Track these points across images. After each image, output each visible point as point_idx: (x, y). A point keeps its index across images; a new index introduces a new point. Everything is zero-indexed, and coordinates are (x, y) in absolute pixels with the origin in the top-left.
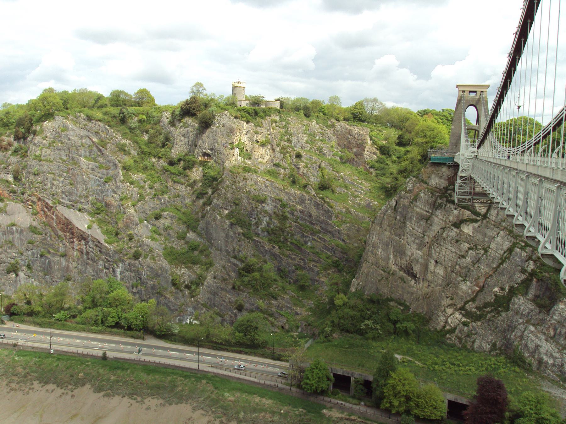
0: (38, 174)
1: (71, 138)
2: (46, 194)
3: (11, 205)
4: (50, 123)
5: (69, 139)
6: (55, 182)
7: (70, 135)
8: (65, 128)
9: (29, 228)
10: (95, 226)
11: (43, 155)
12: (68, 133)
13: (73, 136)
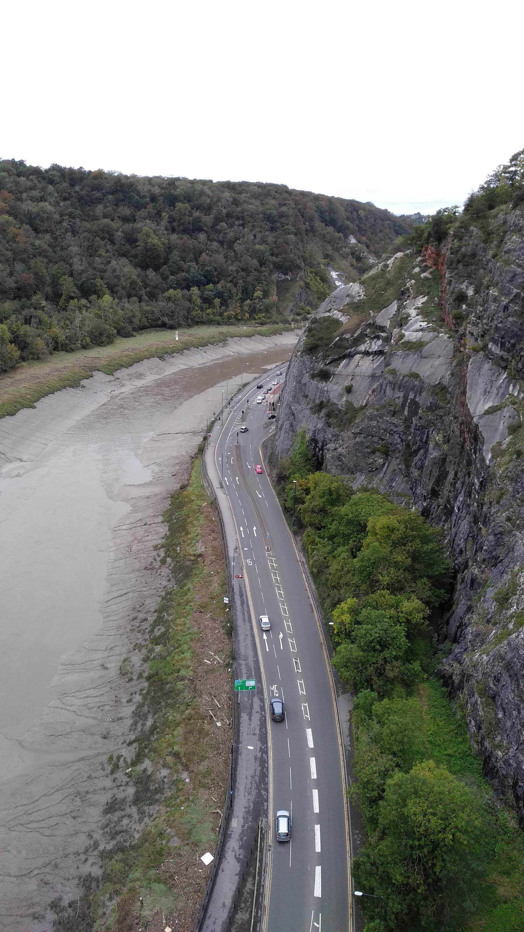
9: (435, 386)
10: (507, 412)
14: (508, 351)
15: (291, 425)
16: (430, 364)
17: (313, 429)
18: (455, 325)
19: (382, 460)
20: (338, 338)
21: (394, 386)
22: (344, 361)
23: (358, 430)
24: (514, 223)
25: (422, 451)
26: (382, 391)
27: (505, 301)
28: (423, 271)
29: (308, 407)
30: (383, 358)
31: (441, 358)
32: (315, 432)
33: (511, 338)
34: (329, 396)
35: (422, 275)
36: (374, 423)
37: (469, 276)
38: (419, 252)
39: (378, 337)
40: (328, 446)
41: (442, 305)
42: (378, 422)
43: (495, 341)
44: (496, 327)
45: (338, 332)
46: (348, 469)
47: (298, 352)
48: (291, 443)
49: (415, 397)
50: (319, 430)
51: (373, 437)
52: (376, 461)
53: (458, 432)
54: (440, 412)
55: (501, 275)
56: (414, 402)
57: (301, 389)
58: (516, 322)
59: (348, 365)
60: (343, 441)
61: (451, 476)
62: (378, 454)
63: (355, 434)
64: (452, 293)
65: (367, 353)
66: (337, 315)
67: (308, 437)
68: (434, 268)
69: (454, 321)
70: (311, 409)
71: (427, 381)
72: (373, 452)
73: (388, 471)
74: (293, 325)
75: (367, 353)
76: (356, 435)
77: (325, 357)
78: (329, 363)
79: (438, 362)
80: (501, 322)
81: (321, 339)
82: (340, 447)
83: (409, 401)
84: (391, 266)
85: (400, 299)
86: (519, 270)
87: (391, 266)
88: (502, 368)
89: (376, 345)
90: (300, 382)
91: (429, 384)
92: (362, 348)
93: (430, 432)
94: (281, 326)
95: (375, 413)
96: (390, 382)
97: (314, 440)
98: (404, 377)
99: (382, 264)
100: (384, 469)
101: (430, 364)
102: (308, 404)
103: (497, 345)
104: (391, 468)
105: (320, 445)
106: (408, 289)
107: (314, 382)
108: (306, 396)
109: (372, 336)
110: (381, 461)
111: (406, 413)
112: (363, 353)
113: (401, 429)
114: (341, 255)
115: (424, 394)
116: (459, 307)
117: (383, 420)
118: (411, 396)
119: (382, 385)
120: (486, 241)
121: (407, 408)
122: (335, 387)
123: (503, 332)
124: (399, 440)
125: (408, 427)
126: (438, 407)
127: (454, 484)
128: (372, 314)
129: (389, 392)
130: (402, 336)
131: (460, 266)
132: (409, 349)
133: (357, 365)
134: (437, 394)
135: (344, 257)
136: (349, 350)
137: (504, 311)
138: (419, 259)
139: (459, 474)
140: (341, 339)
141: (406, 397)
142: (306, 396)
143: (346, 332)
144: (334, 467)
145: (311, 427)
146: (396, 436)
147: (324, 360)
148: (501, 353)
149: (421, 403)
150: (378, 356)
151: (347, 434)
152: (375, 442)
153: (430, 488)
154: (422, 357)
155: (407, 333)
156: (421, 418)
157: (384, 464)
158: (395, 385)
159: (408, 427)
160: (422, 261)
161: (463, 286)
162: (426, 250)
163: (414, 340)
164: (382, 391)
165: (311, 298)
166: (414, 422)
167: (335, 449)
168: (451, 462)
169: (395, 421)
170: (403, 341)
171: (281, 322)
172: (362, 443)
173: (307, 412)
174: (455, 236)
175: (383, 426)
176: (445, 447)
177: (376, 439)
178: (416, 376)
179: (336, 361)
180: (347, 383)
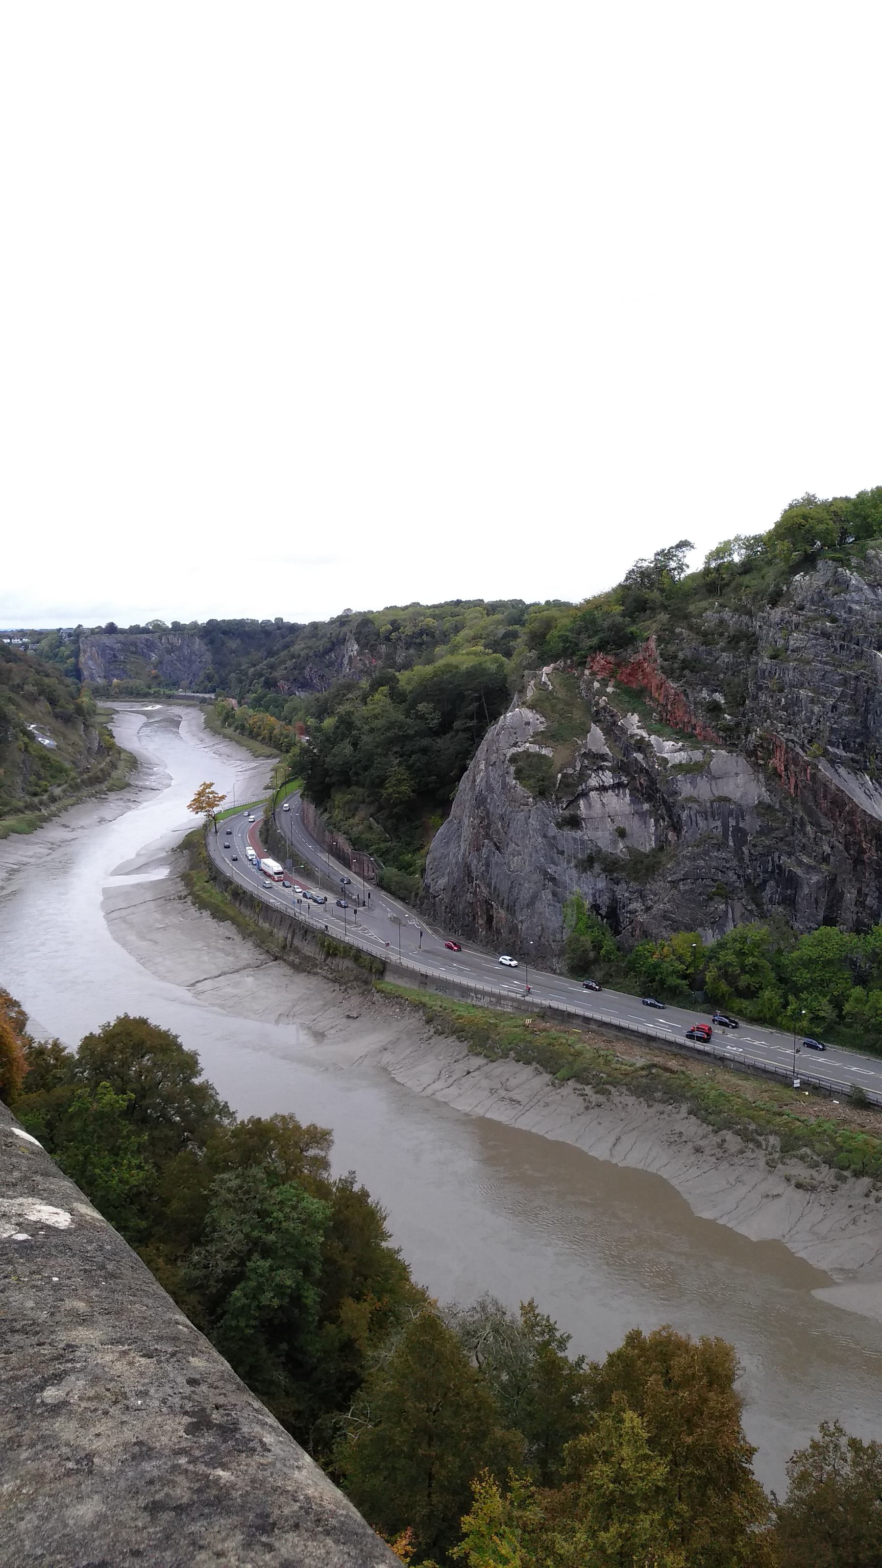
0: (781, 690)
1: (857, 607)
2: (795, 734)
3: (721, 758)
4: (807, 578)
5: (850, 610)
6: (816, 709)
7: (853, 602)
8: (842, 585)
9: (756, 807)
11: (791, 648)
12: (848, 597)
13: (857, 602)
14: (856, 752)
15: (554, 894)
16: (732, 786)
17: (591, 892)
18: (724, 739)
19: (723, 906)
20: (560, 775)
21: (705, 815)
22: (581, 802)
23: (675, 877)
24: (782, 620)
25: (772, 883)
26: (694, 824)
27: (831, 701)
28: (607, 686)
29: (572, 865)
30: (627, 791)
31: (741, 775)
32: (594, 895)
33: (856, 738)
34: (597, 846)
35: (610, 690)
36: (702, 863)
37: (705, 683)
38: (582, 664)
39: (601, 768)
40: (631, 907)
41: (667, 720)
42: (704, 860)
43: (832, 745)
44: (832, 730)
45: (553, 770)
46: (686, 927)
47: (528, 798)
48: (562, 917)
49: (737, 823)
50: (600, 891)
51: (703, 879)
52: (716, 908)
53: (841, 847)
54: (777, 834)
55: (802, 675)
56: (737, 829)
57: (552, 846)
58: (855, 721)
59: (589, 806)
60: (655, 895)
61: (850, 896)
62: (717, 898)
63: (673, 882)
64: (695, 704)
65: (603, 789)
66: (535, 748)
67: (587, 904)
68: (613, 680)
69: (721, 734)
70: (576, 866)
71: (743, 802)
72: (711, 899)
73: (736, 917)
74: (43, 811)
75: (603, 789)
76: (674, 884)
77: (558, 800)
78: (567, 807)
79: (740, 780)
80: (835, 723)
81: (543, 780)
82: (655, 903)
83: (731, 829)
84: (549, 683)
85: (597, 721)
86: (828, 668)
87: (549, 683)
88: (858, 770)
89: (608, 778)
90: (545, 836)
91: (747, 805)
92: (593, 782)
93: (776, 859)
94: (29, 815)
95: (696, 850)
96: (698, 812)
97: (595, 907)
98: (712, 802)
99: (533, 682)
100: (730, 915)
101: (732, 786)
102: (569, 862)
103: (838, 747)
104: (738, 914)
105: (604, 911)
106: (604, 708)
107: (569, 833)
108: (562, 853)
109: (595, 768)
110: (722, 907)
111: (731, 843)
112: (597, 789)
113: (735, 863)
114: (23, 696)
115: (747, 818)
116: (718, 718)
117: (710, 857)
118: (732, 822)
119: (690, 817)
120: (705, 643)
121: (730, 838)
122: (599, 833)
123: (843, 733)
124: (735, 877)
125: (741, 860)
126: (772, 830)
127: (860, 903)
128: (580, 742)
129: (702, 823)
130: (665, 760)
131: (687, 672)
132: (688, 772)
133: (603, 805)
134: (763, 815)
135: (33, 699)
136: (580, 788)
137: (832, 712)
138: (587, 672)
139: (866, 890)
140: (565, 776)
141: (725, 826)
142: (562, 853)
143: (563, 767)
144: (662, 930)
145: (587, 889)
146: (731, 873)
147: (558, 804)
148: (850, 755)
149: (747, 828)
150: (619, 790)
151: (658, 885)
152: (708, 886)
153: (820, 918)
154: (715, 778)
155: (665, 755)
156: (755, 846)
157: (727, 910)
158: (706, 813)
159: (741, 860)
160: (593, 674)
161: (704, 694)
162: (593, 660)
163: (684, 762)
164: (694, 824)
165: (35, 767)
166: (746, 851)
167: (648, 909)
168: (844, 880)
169: (724, 855)
170: (670, 765)
171: (26, 807)
172: (692, 890)
173: (574, 872)
174: (660, 640)
175: (714, 864)
176: (824, 867)
177: (709, 882)
178: (727, 800)
179: (573, 803)
180: (610, 826)
